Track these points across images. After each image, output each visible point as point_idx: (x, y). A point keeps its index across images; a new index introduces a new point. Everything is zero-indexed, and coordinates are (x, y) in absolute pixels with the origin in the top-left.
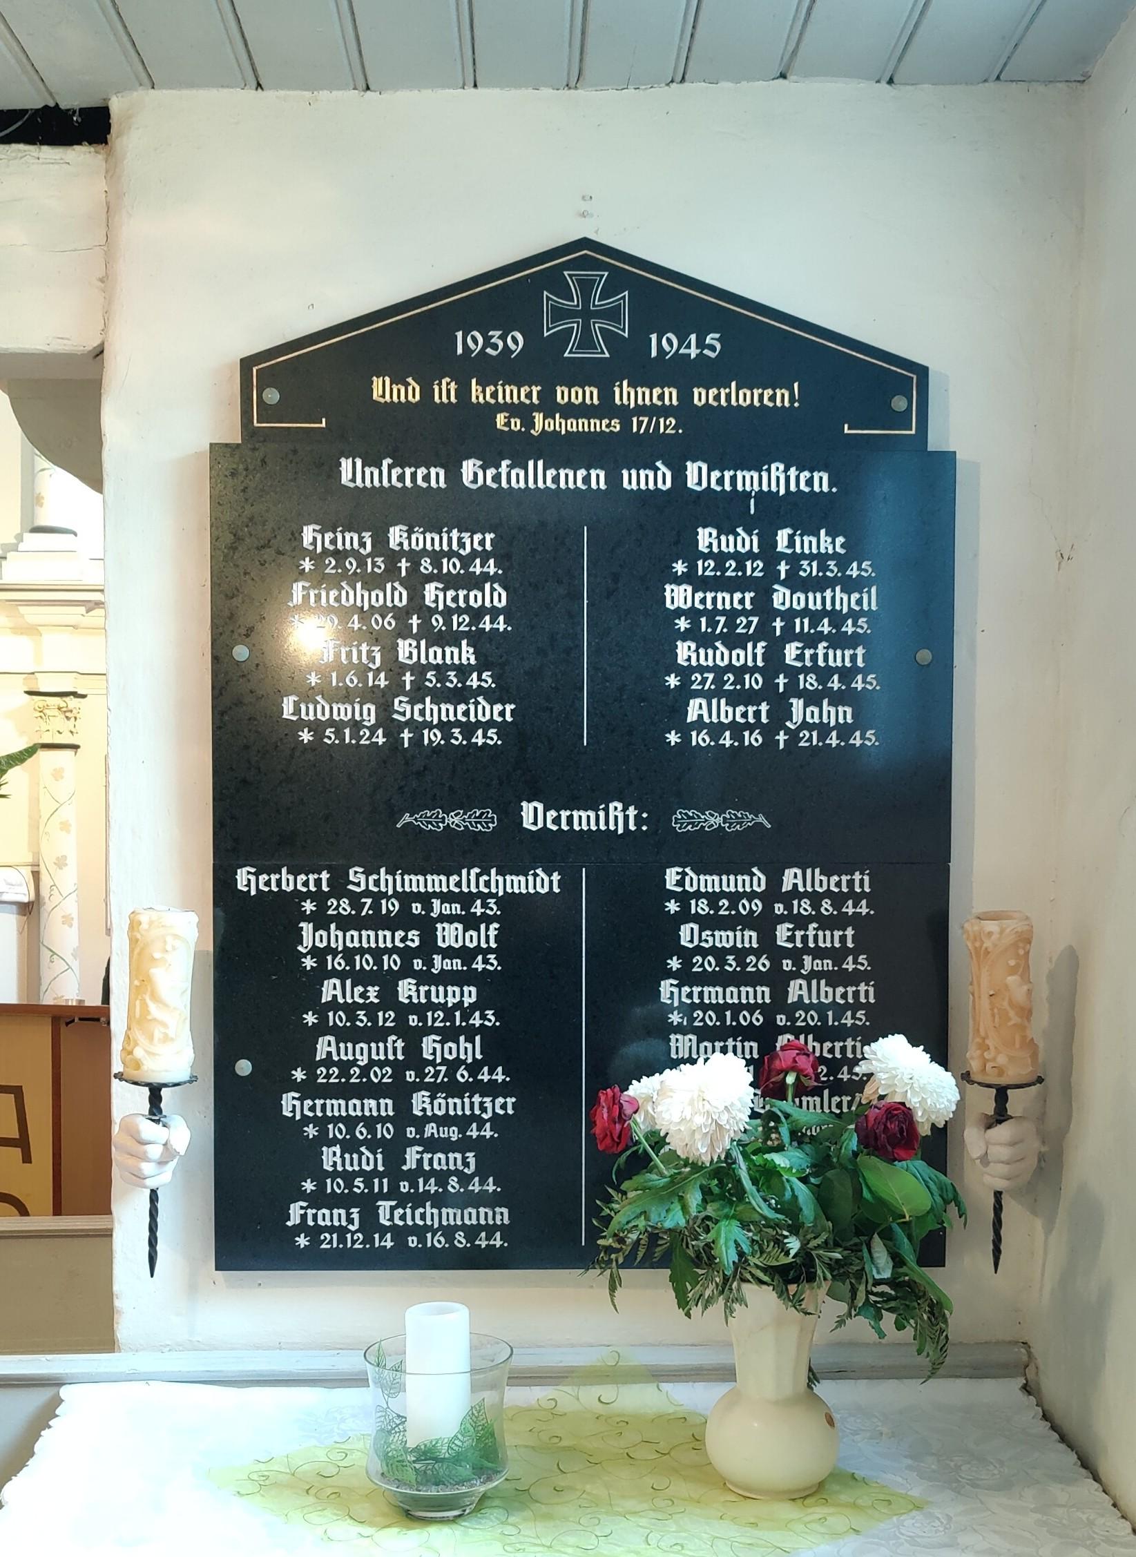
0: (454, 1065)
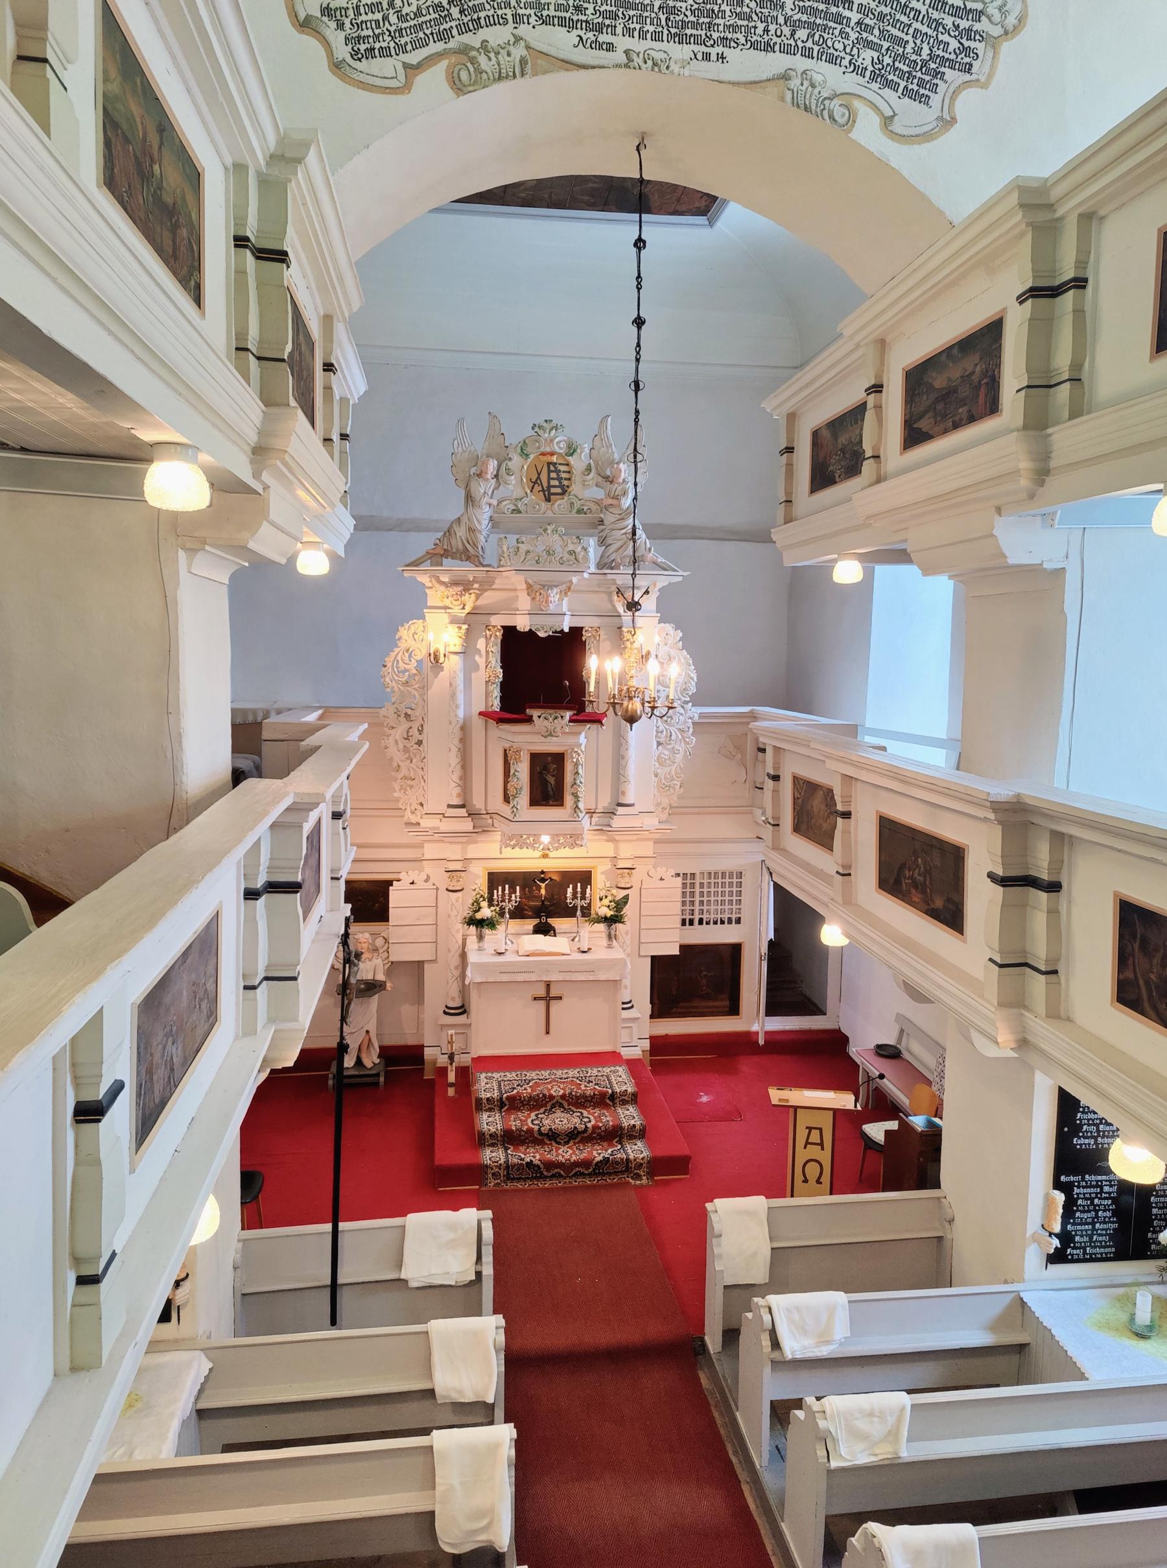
0: (1105, 1217)
